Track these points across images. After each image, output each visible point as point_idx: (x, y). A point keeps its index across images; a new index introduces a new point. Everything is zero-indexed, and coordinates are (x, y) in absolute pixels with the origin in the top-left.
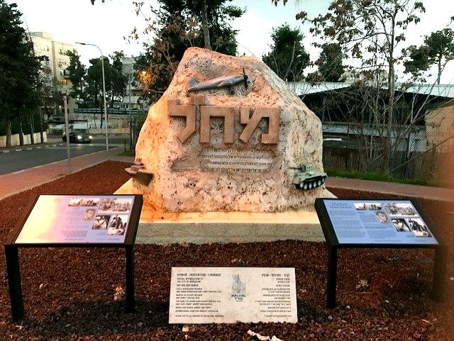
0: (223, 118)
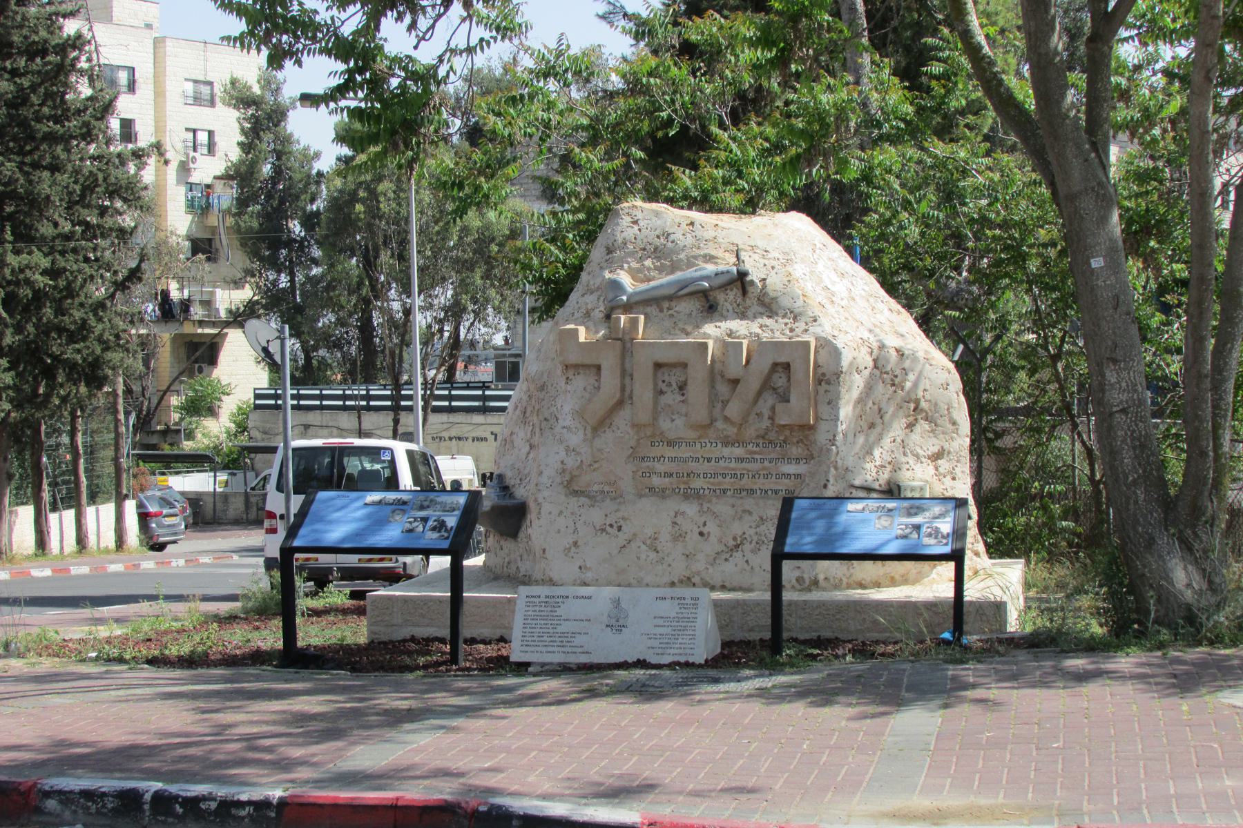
0: (685, 366)
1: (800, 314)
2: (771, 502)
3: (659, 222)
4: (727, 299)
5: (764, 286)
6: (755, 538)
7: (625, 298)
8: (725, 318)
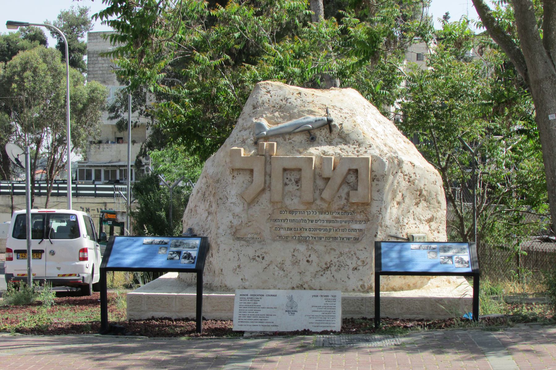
0: (300, 170)
1: (362, 143)
2: (346, 244)
3: (281, 92)
4: (321, 134)
5: (342, 128)
6: (337, 264)
7: (265, 133)
8: (321, 145)
